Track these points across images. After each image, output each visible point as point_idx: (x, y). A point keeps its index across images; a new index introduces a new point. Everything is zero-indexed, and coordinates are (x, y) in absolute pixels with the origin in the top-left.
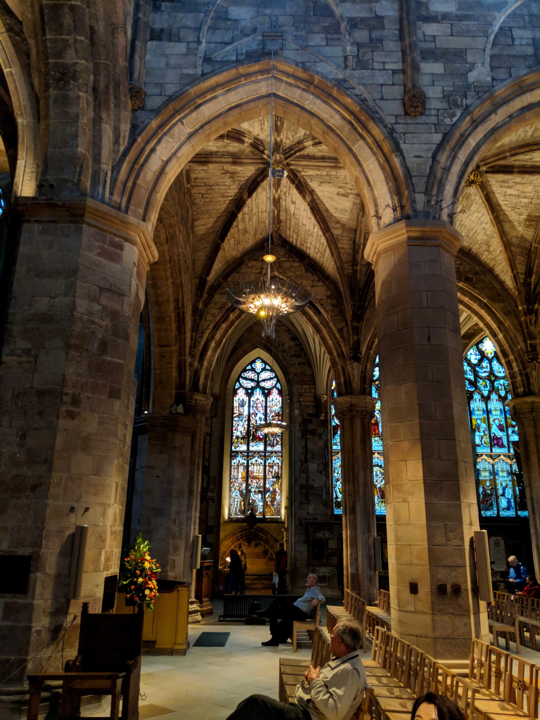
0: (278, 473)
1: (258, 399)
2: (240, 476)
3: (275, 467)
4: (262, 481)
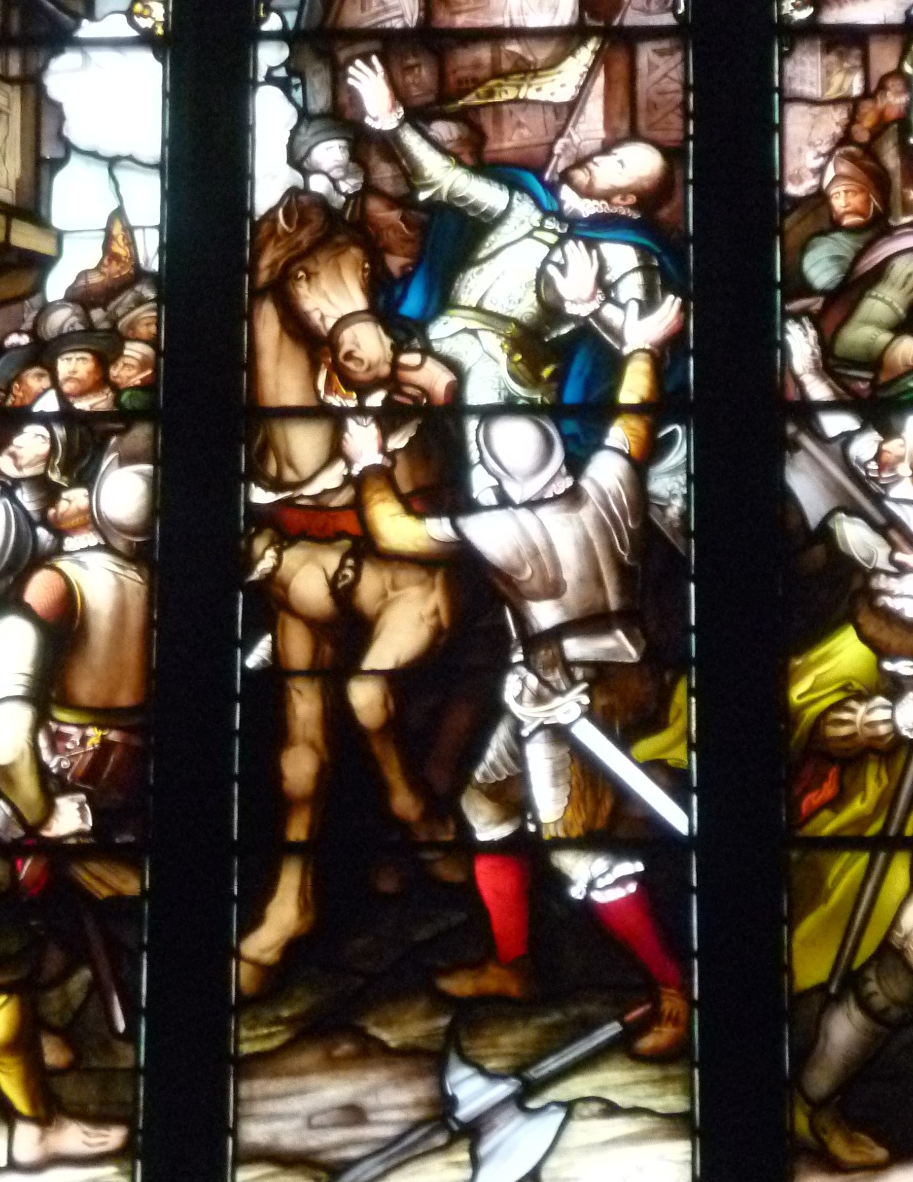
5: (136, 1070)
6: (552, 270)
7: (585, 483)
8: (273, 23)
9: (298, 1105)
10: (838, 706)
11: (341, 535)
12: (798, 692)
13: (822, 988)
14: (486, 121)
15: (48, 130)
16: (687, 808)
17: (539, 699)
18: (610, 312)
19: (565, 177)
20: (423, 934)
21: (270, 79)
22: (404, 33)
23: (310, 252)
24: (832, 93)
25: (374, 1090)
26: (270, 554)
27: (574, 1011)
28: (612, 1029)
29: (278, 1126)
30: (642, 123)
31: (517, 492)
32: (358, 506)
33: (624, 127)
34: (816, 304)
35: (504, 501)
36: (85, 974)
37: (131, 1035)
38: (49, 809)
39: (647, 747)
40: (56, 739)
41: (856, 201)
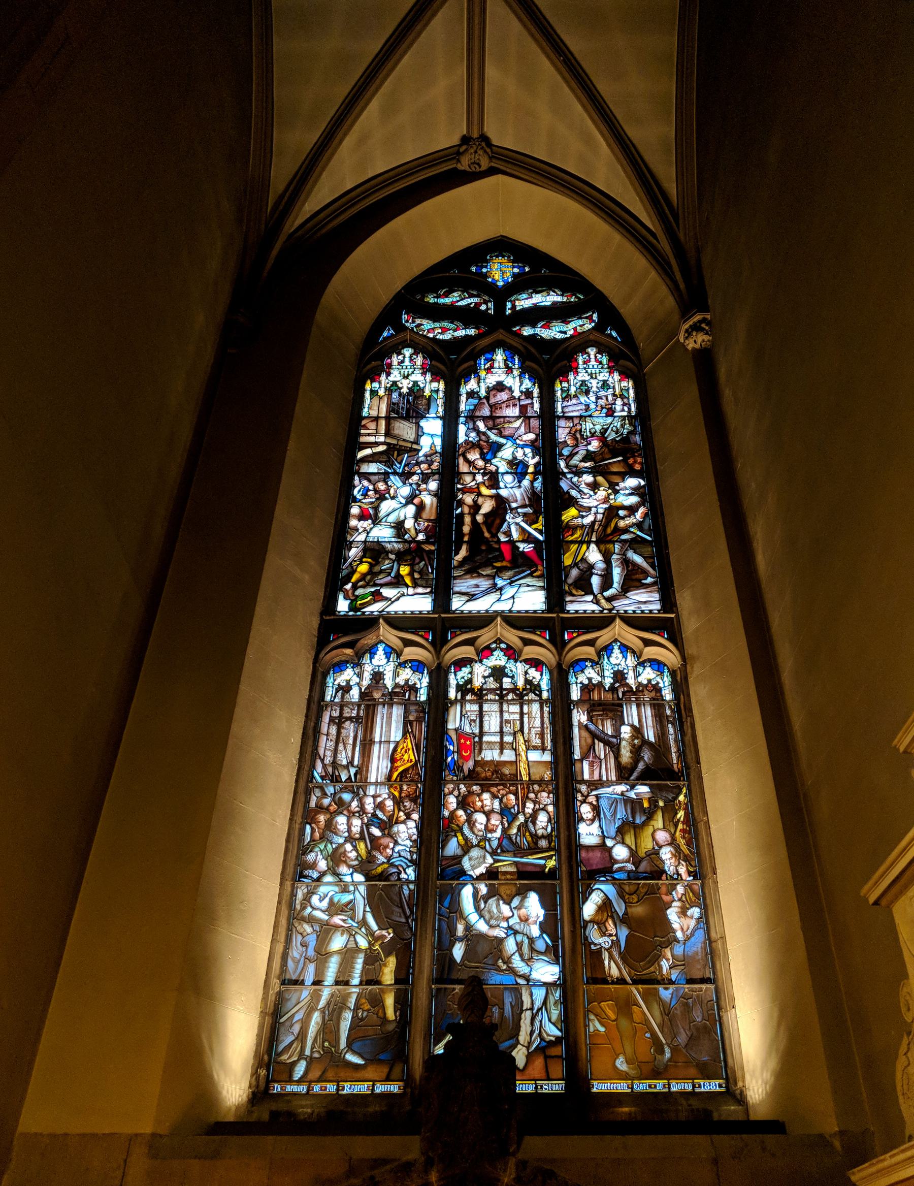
0: (660, 748)
1: (500, 387)
2: (379, 767)
3: (631, 714)
4: (546, 798)
8: (463, 415)
9: (465, 584)
12: (563, 518)
14: (502, 430)
15: (420, 430)
17: (513, 518)
18: (526, 459)
19: (517, 438)
22: (487, 417)
23: (469, 449)
28: (529, 572)
31: (508, 486)
32: (478, 488)
35: (506, 487)
36: (424, 562)
37: (432, 573)
38: (417, 535)
39: (534, 526)
40: (418, 524)
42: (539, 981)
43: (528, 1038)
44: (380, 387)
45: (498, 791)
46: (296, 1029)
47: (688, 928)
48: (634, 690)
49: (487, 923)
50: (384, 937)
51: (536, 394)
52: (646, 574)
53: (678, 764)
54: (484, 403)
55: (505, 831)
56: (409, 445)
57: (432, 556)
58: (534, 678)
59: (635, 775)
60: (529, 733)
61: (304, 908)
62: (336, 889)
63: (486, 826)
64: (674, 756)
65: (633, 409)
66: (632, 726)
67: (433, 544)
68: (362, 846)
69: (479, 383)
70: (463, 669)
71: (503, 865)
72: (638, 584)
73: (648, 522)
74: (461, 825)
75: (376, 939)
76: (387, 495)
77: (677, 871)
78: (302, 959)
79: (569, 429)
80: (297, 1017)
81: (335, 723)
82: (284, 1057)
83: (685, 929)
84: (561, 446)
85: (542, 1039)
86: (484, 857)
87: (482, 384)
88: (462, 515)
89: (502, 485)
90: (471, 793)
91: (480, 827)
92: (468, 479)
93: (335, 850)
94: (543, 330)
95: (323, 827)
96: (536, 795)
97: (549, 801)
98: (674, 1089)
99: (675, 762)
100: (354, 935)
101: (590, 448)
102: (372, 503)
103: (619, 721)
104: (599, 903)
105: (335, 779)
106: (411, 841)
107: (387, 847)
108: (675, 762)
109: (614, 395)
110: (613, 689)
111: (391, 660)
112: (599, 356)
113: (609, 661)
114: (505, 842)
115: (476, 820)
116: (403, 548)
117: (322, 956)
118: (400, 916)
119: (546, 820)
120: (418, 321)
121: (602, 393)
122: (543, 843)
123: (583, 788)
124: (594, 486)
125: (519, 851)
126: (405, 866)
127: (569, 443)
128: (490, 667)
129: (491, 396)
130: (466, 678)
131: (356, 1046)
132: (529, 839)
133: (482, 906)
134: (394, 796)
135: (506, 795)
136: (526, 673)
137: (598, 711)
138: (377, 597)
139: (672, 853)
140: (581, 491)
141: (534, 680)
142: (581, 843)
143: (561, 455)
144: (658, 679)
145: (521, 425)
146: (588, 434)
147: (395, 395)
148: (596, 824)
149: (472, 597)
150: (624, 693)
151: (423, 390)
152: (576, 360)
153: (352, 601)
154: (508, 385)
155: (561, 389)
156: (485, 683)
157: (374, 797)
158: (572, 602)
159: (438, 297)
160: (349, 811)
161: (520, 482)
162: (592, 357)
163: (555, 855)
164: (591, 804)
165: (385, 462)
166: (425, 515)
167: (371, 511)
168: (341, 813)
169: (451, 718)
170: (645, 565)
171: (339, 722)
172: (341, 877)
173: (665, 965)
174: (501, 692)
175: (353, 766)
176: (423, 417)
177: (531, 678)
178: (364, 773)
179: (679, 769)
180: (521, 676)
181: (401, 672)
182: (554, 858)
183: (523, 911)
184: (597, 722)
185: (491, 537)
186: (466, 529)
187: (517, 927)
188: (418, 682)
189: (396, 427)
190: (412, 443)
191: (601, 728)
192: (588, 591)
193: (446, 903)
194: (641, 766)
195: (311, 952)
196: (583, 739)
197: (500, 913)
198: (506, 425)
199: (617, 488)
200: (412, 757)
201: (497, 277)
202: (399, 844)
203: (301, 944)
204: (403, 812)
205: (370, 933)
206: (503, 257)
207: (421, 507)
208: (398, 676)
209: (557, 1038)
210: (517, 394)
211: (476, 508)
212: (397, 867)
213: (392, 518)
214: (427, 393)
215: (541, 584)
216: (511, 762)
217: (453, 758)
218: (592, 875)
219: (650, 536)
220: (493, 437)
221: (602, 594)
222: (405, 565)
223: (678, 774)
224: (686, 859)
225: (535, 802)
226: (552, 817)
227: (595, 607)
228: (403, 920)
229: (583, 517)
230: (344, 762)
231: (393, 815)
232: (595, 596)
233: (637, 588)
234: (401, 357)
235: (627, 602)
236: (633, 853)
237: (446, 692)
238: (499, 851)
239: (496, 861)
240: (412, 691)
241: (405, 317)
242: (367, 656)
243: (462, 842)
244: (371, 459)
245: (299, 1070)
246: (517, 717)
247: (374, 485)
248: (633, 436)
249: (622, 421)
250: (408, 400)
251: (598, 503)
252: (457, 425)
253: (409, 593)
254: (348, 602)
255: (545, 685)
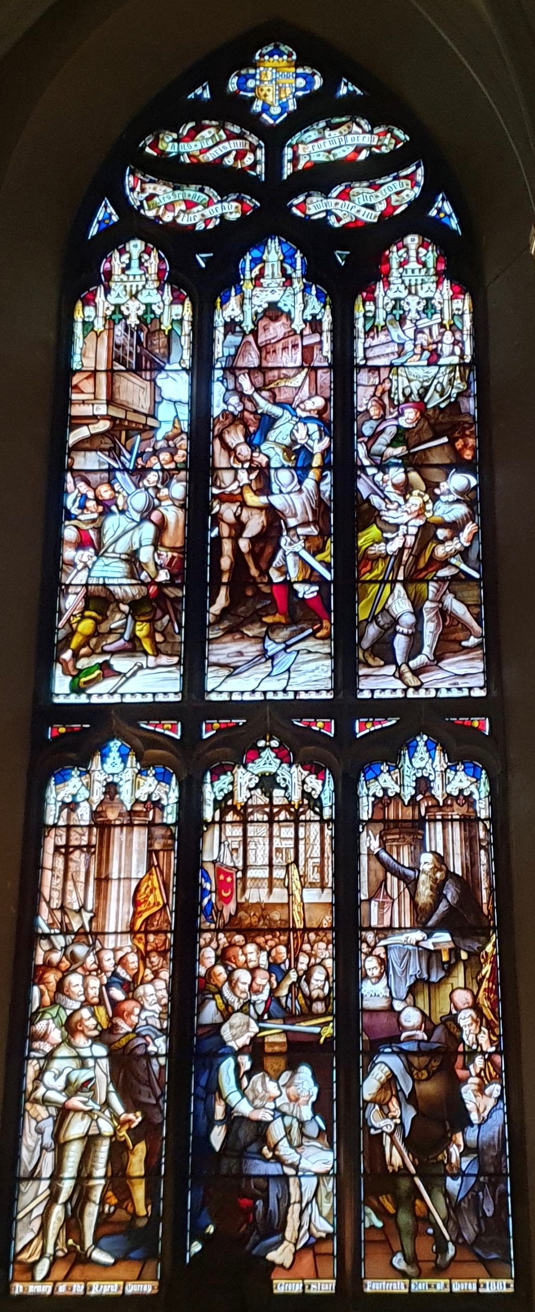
1: (273, 312)
3: (435, 836)
4: (324, 951)
5: (181, 642)
6: (294, 431)
7: (303, 488)
8: (218, 365)
10: (372, 545)
11: (237, 501)
12: (360, 542)
13: (366, 620)
14: (276, 391)
16: (330, 572)
17: (290, 544)
18: (310, 442)
20: (259, 606)
21: (218, 380)
22: (255, 368)
24: (370, 383)
25: (245, 647)
26: (218, 507)
27: (300, 626)
28: (310, 631)
29: (219, 657)
30: (319, 392)
31: (283, 489)
32: (241, 494)
33: (314, 393)
34: (366, 439)
35: (281, 492)
36: (167, 617)
37: (180, 633)
39: (320, 557)
40: (159, 555)
41: (377, 412)
42: (309, 1171)
43: (296, 1234)
44: (96, 316)
45: (266, 942)
46: (36, 1225)
47: (485, 1109)
48: (441, 804)
49: (251, 1103)
50: (130, 1121)
51: (326, 326)
52: (466, 628)
53: (488, 903)
54: (249, 343)
55: (272, 991)
56: (142, 420)
57: (179, 607)
58: (313, 789)
59: (435, 918)
60: (305, 866)
61: (35, 1089)
62: (74, 1063)
63: (250, 986)
64: (484, 893)
65: (468, 351)
66: (435, 853)
67: (179, 587)
68: (101, 1011)
69: (242, 305)
70: (222, 777)
71: (271, 1035)
72: (457, 647)
73: (477, 548)
74: (220, 985)
75: (122, 1124)
76: (114, 508)
77: (477, 1040)
78: (38, 1148)
79: (373, 389)
80: (35, 1213)
81: (61, 853)
82: (24, 1256)
83: (481, 1110)
84: (360, 419)
85: (311, 1235)
86: (248, 1025)
87: (247, 308)
88: (219, 539)
89: (275, 488)
90: (232, 945)
91: (243, 987)
92: (227, 476)
93: (70, 1017)
94: (340, 202)
95: (54, 989)
96: (312, 947)
97: (327, 954)
98: (456, 1289)
99: (485, 901)
100: (96, 1120)
101: (403, 422)
102: (94, 521)
103: (419, 845)
104: (382, 1080)
105: (65, 931)
106: (161, 1005)
107: (131, 1013)
108: (485, 901)
109: (442, 325)
110: (413, 802)
111: (129, 765)
112: (423, 251)
113: (411, 763)
114: (273, 1005)
115: (238, 980)
116: (139, 593)
117: (60, 1147)
118: (149, 1097)
119: (323, 977)
120: (150, 189)
121: (424, 323)
122: (319, 1007)
123: (370, 936)
124: (405, 489)
125: (289, 1016)
126: (154, 1036)
127: (372, 413)
128: (257, 775)
129: (261, 331)
130: (226, 792)
131: (103, 1242)
132: (303, 1002)
133: (245, 1082)
134: (138, 949)
135: (276, 946)
136: (304, 782)
137: (393, 834)
138: (106, 670)
139: (472, 1018)
140: (386, 497)
141: (313, 793)
142: (364, 1006)
143: (361, 434)
144: (473, 788)
145: (303, 383)
146: (402, 399)
147: (119, 329)
148: (384, 981)
149: (233, 670)
150: (427, 808)
151: (158, 319)
152: (388, 260)
153: (74, 677)
154: (286, 309)
155: (365, 316)
156: (251, 797)
157: (115, 950)
158: (367, 676)
159: (178, 141)
160: (85, 970)
161: (300, 482)
162: (413, 253)
163: (332, 1021)
164: (378, 957)
165: (109, 450)
166: (167, 541)
167: (92, 534)
168: (74, 971)
169: (207, 847)
170: (468, 618)
171: (65, 851)
172: (78, 1050)
173: (455, 1151)
174: (271, 810)
175: (86, 911)
176: (161, 369)
177: (309, 790)
178: (100, 920)
179: (489, 911)
180: (297, 787)
181: (142, 781)
182: (331, 1024)
183: (292, 1090)
184: (391, 850)
185: (260, 575)
186: (226, 563)
187: (285, 1109)
188: (164, 797)
189: (121, 390)
190: (147, 416)
191: (395, 857)
192: (390, 659)
193: (203, 1082)
194: (443, 907)
195: (48, 1140)
196: (372, 874)
197: (266, 1092)
198: (282, 384)
199: (437, 491)
200: (160, 900)
201: (270, 99)
202: (146, 1010)
203: (36, 1131)
204: (150, 969)
205: (115, 1117)
206: (281, 54)
207: (161, 527)
208: (139, 787)
209: (328, 1235)
210: (298, 325)
211: (239, 526)
212: (144, 1037)
213: (122, 547)
214: (166, 325)
215: (327, 650)
216: (282, 905)
217: (210, 900)
218: (374, 1050)
219: (478, 571)
220: (265, 406)
221: (407, 664)
222: (143, 621)
223: (487, 917)
224: (490, 1027)
225: (310, 956)
226: (331, 974)
227: (399, 685)
228: (154, 1102)
229: (387, 541)
230: (76, 907)
231: (138, 973)
232: (398, 667)
233: (455, 653)
234: (125, 258)
235: (440, 675)
236: (425, 1018)
237: (200, 811)
238: (266, 1017)
239: (262, 1029)
240: (157, 809)
241: (129, 180)
242: (97, 759)
243: (222, 1007)
244: (87, 445)
245: (42, 1270)
246: (291, 843)
247: (95, 490)
248: (465, 400)
249: (450, 372)
250: (138, 338)
251: (410, 517)
252: (209, 381)
253: (150, 665)
254: (70, 678)
255: (328, 800)
